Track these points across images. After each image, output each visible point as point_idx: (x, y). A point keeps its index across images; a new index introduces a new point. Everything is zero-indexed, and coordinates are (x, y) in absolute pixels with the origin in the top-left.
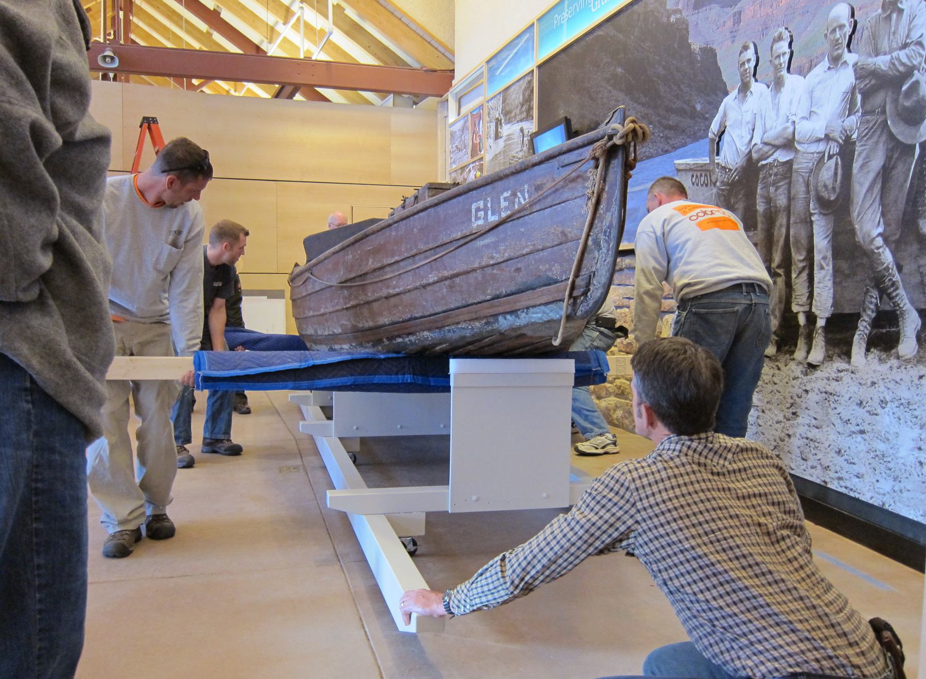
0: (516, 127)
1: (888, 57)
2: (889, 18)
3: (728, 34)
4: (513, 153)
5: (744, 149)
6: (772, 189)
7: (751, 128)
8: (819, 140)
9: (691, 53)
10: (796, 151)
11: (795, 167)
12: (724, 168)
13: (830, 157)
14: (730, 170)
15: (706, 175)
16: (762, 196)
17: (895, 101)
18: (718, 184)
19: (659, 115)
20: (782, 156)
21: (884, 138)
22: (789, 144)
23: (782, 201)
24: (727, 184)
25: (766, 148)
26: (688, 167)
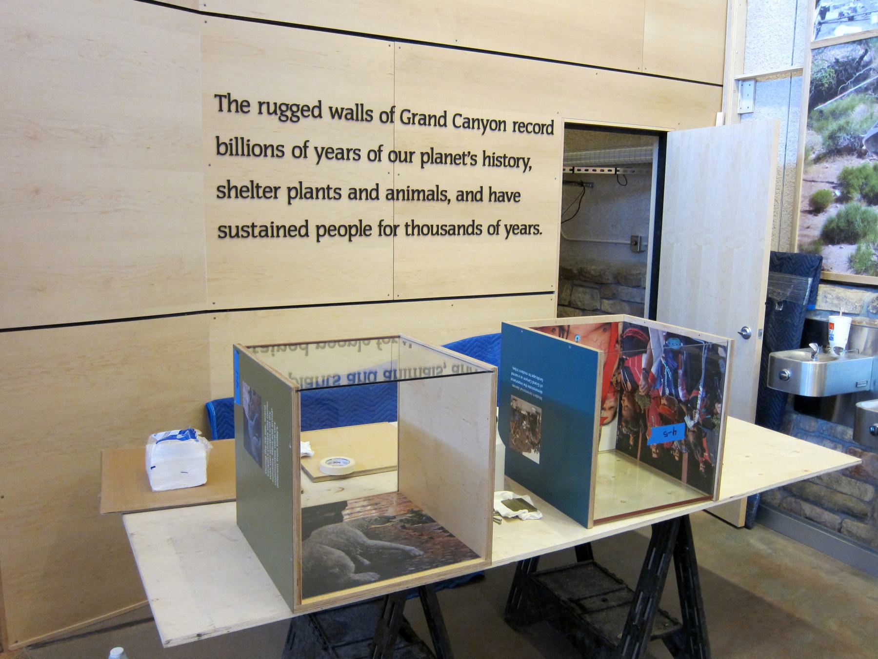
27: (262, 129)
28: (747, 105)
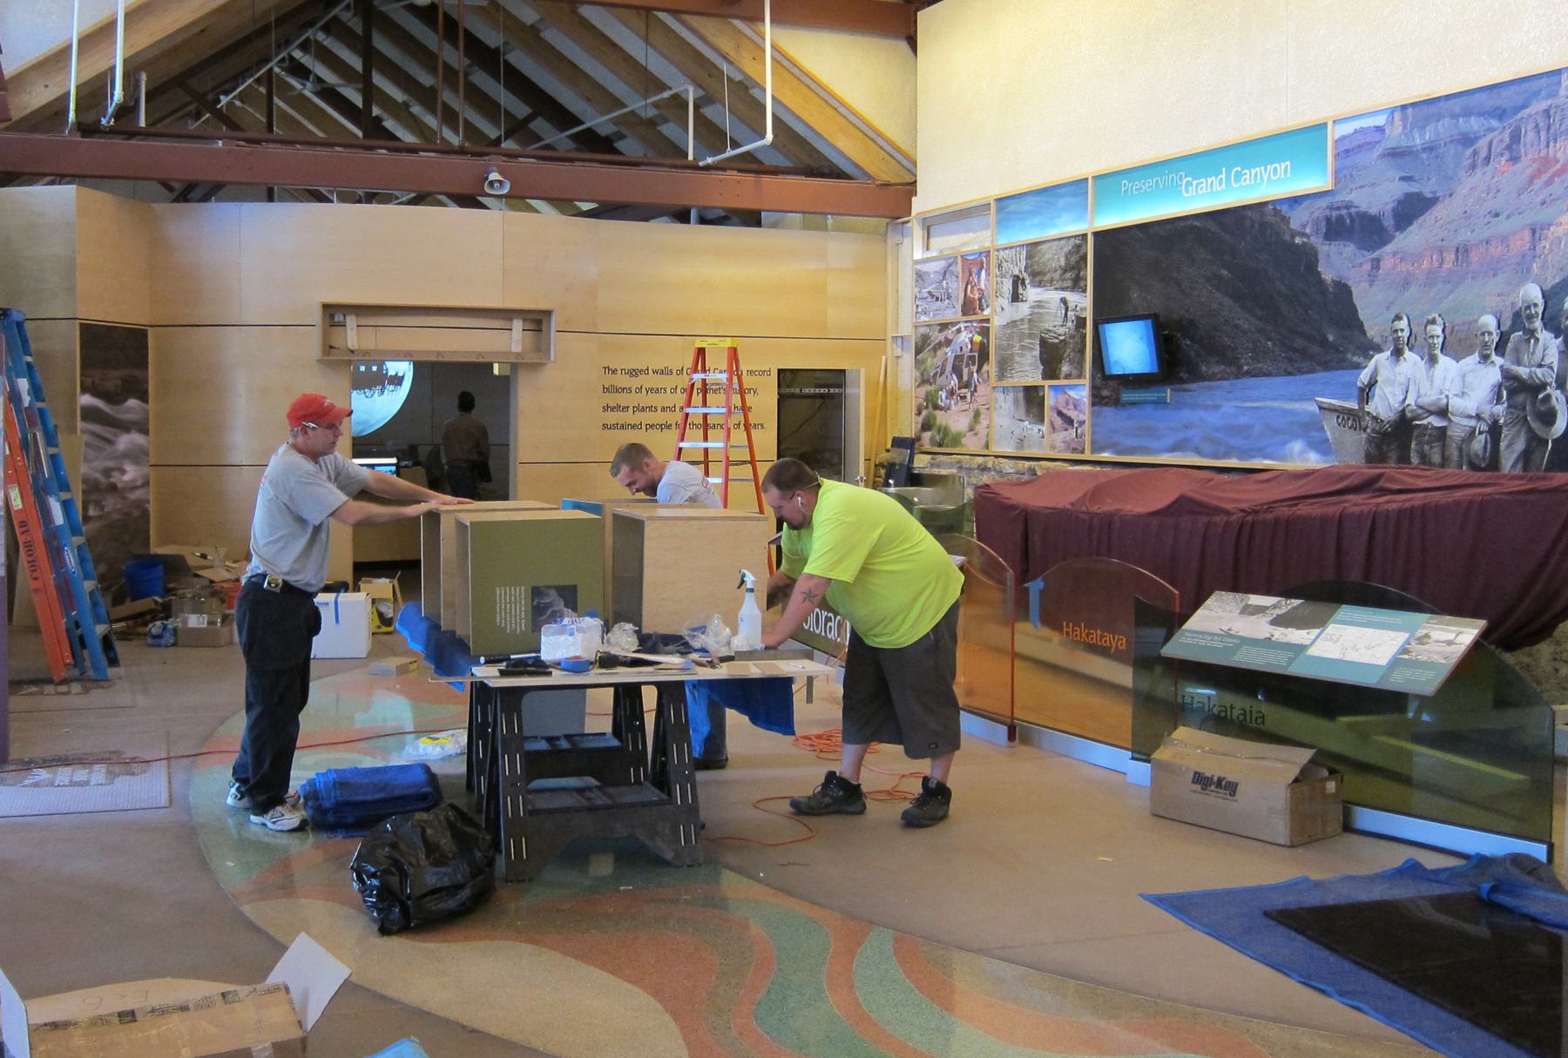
0: (1052, 296)
2: (1528, 341)
4: (1048, 326)
5: (1397, 406)
6: (1426, 447)
8: (1470, 417)
9: (1321, 282)
12: (1375, 418)
17: (1534, 403)
20: (1436, 422)
22: (1443, 412)
27: (622, 380)
28: (898, 352)
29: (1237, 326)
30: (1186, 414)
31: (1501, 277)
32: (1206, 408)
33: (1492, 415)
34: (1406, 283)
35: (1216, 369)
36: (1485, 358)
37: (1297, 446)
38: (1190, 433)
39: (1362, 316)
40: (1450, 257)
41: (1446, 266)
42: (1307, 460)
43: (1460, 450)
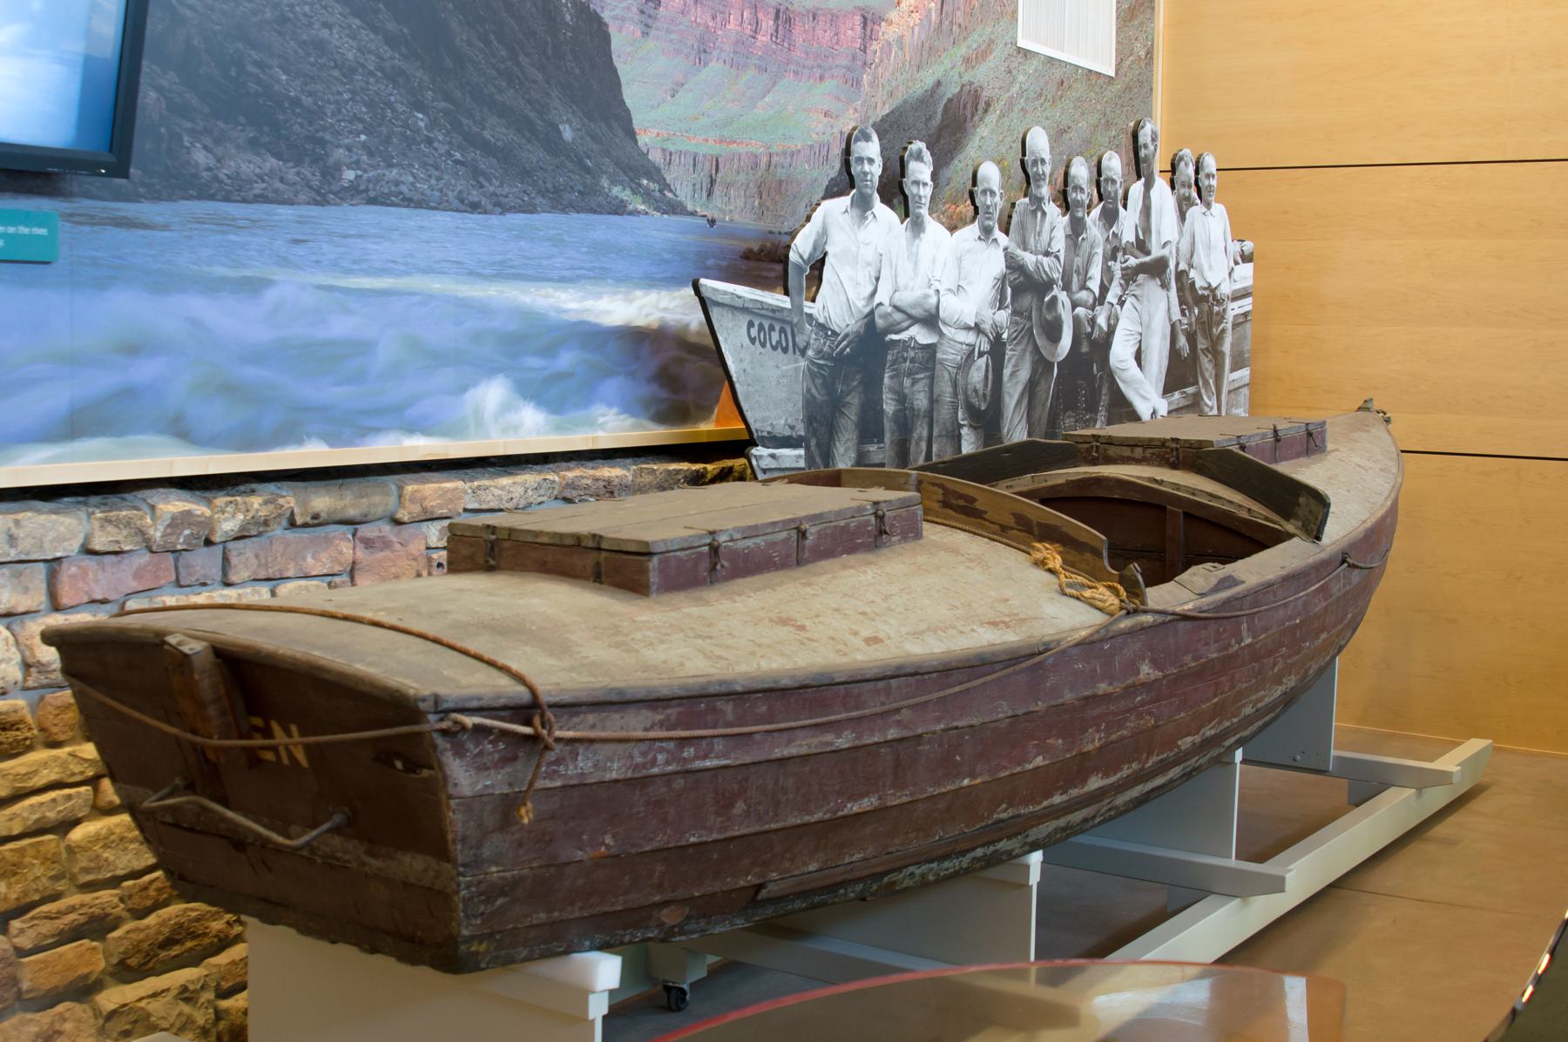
1: (1033, 258)
2: (1034, 213)
3: (635, 10)
5: (861, 306)
6: (907, 382)
7: (874, 274)
8: (968, 328)
10: (941, 334)
11: (939, 355)
12: (822, 327)
13: (981, 354)
14: (835, 333)
15: (782, 330)
16: (892, 390)
17: (1040, 310)
18: (810, 353)
19: (448, 97)
20: (921, 335)
21: (1030, 348)
23: (921, 401)
24: (828, 357)
25: (898, 316)
26: (739, 303)
29: (320, 46)
30: (126, 308)
31: (829, 85)
32: (212, 287)
33: (995, 325)
34: (703, 52)
35: (246, 164)
36: (987, 231)
37: (493, 393)
38: (145, 371)
39: (630, 95)
40: (768, 24)
41: (763, 38)
42: (516, 428)
43: (955, 385)
